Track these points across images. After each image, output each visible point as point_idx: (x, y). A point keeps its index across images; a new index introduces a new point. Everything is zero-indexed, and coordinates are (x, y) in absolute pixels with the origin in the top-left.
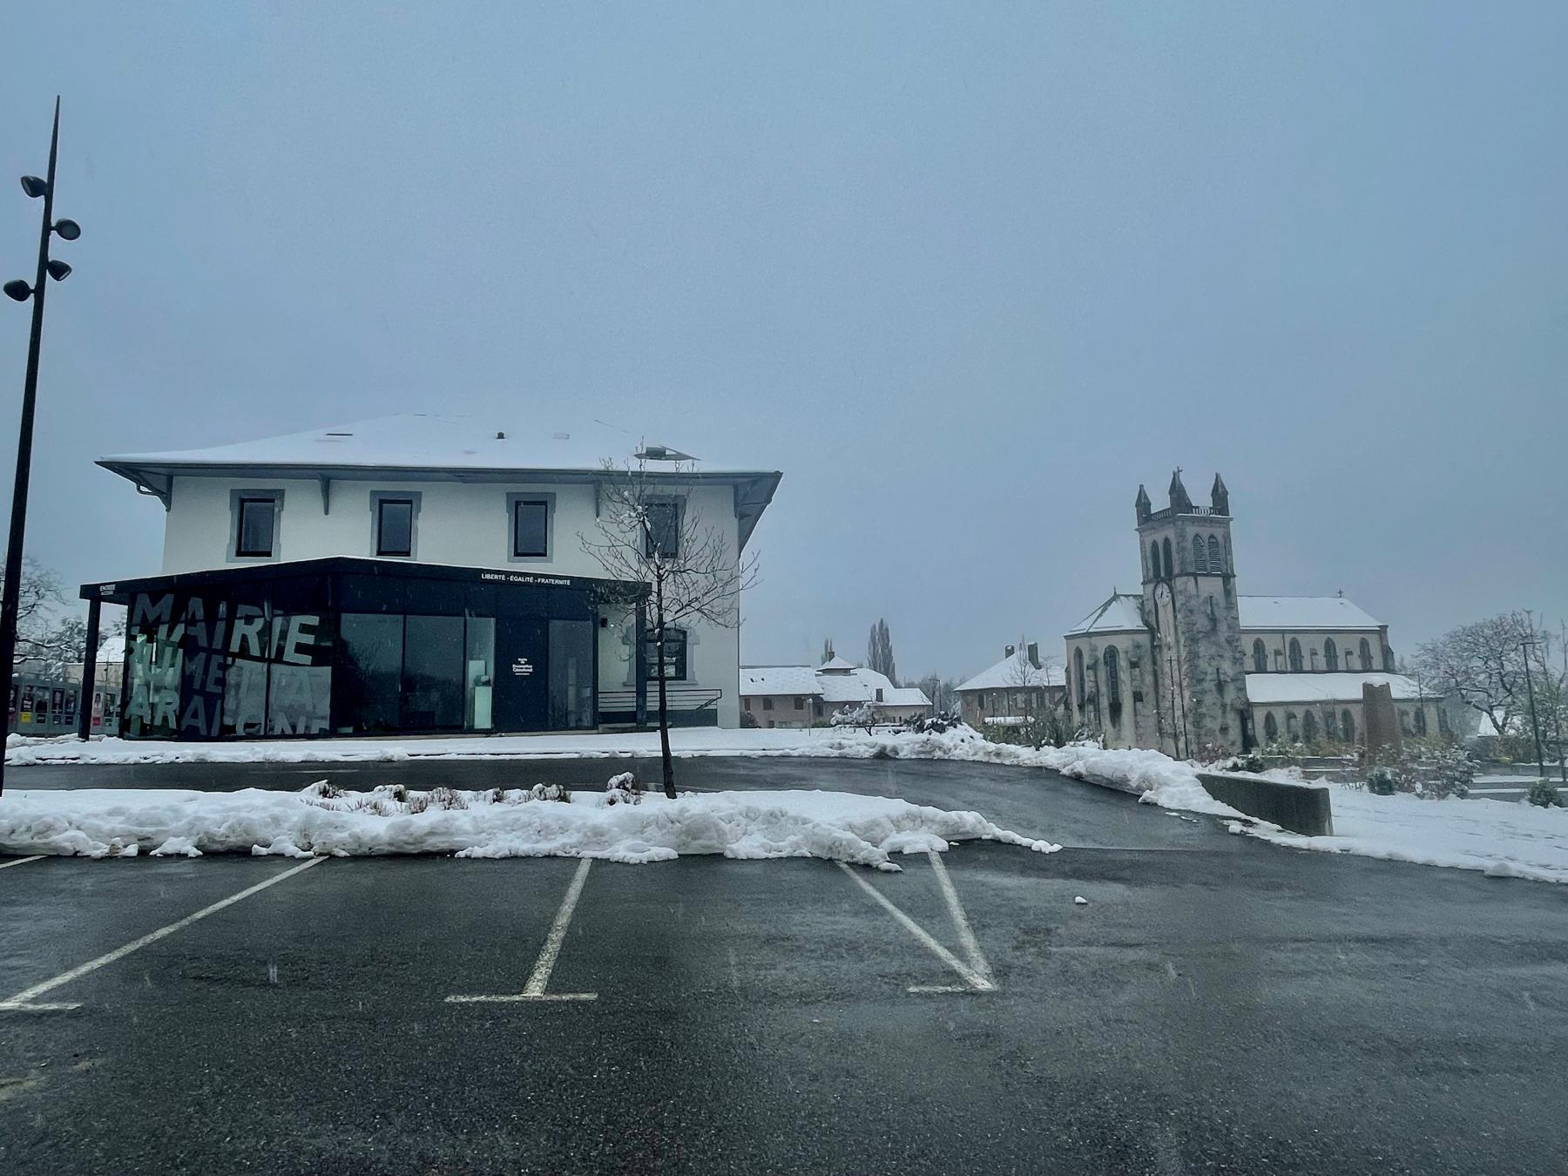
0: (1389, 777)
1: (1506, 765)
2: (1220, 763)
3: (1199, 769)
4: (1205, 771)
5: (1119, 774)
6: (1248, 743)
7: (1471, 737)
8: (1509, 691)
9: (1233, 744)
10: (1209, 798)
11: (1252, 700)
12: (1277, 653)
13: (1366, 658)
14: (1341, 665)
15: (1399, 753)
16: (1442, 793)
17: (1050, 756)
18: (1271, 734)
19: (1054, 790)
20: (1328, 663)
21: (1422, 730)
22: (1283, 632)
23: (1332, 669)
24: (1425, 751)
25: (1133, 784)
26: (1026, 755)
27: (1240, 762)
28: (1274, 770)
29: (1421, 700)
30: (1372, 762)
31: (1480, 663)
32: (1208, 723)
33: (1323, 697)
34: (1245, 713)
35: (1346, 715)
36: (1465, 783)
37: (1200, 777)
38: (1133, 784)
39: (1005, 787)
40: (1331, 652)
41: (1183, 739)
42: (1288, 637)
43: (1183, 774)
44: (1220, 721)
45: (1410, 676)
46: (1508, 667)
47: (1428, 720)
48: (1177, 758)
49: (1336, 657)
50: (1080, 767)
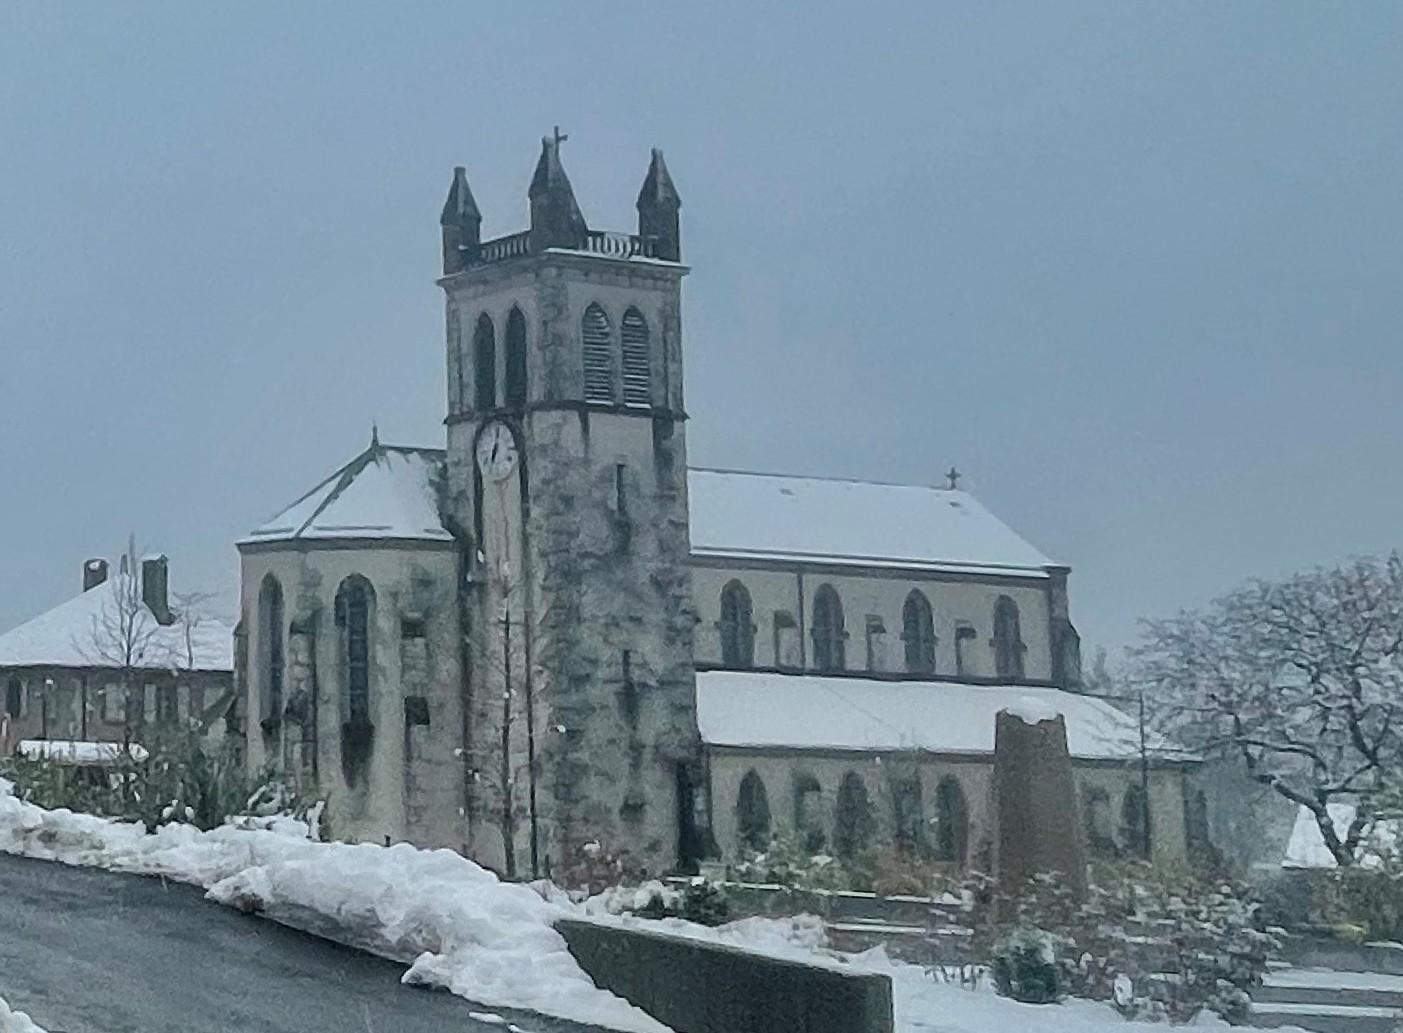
0: (1049, 956)
1: (1350, 945)
2: (617, 895)
3: (563, 906)
4: (578, 914)
5: (356, 907)
6: (693, 847)
7: (1266, 868)
8: (1372, 755)
9: (654, 847)
10: (585, 984)
11: (709, 738)
12: (782, 621)
13: (1008, 645)
14: (944, 662)
15: (1079, 896)
16: (1182, 1004)
17: (183, 850)
18: (754, 829)
19: (188, 937)
20: (911, 656)
21: (1141, 840)
22: (800, 568)
23: (919, 670)
24: (1148, 897)
25: (392, 934)
26: (120, 842)
27: (669, 895)
28: (754, 922)
29: (1143, 764)
30: (1008, 916)
31: (1301, 679)
32: (593, 789)
33: (891, 742)
34: (689, 769)
35: (949, 791)
36: (1244, 983)
37: (564, 927)
38: (392, 934)
39: (62, 921)
40: (919, 625)
41: (525, 827)
42: (813, 583)
43: (520, 915)
44: (623, 786)
45: (1120, 701)
46: (1373, 695)
47: (1158, 818)
48: (508, 876)
49: (932, 640)
50: (257, 883)
